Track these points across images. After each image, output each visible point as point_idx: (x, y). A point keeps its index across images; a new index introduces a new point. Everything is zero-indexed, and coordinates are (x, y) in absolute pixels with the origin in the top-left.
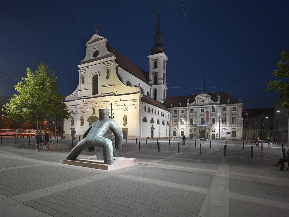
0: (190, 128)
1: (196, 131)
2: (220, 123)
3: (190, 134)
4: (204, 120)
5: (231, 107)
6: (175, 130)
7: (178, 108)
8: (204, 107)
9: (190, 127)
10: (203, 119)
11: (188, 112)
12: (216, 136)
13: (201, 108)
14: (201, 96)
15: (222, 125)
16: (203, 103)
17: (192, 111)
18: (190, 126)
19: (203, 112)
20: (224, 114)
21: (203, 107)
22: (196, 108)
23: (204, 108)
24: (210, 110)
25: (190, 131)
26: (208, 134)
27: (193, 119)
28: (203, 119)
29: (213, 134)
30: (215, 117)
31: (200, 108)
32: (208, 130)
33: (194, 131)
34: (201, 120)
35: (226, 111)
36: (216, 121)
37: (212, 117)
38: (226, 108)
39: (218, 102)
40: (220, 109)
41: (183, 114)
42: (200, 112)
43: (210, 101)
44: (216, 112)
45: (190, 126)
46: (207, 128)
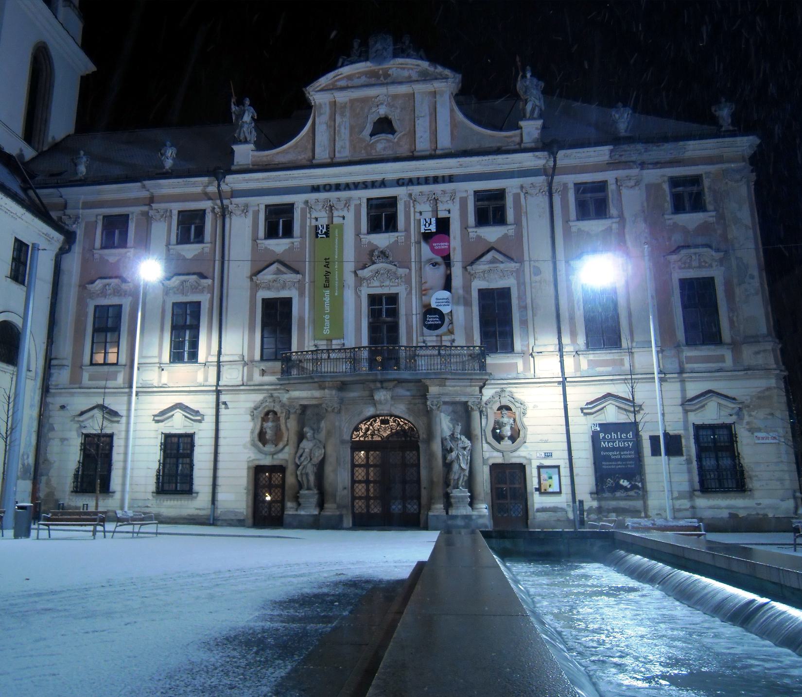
0: (259, 397)
1: (322, 435)
2: (566, 340)
3: (258, 471)
5: (652, 175)
6: (95, 424)
7: (133, 190)
8: (400, 183)
9: (257, 388)
10: (393, 299)
11: (243, 231)
12: (533, 482)
13: (365, 185)
14: (363, 80)
15: (584, 362)
16: (382, 144)
17: (279, 221)
18: (257, 378)
19: (391, 225)
21: (383, 184)
22: (315, 189)
23: (400, 192)
25: (261, 436)
26: (448, 466)
28: (393, 299)
29: (497, 458)
30: (509, 282)
31: (356, 186)
32: (445, 424)
33: (301, 437)
34: (374, 314)
36: (524, 323)
37: (478, 284)
38: (612, 187)
39: (531, 129)
40: (557, 199)
42: (358, 234)
43: (454, 125)
44: (518, 223)
45: (257, 378)
46: (433, 390)
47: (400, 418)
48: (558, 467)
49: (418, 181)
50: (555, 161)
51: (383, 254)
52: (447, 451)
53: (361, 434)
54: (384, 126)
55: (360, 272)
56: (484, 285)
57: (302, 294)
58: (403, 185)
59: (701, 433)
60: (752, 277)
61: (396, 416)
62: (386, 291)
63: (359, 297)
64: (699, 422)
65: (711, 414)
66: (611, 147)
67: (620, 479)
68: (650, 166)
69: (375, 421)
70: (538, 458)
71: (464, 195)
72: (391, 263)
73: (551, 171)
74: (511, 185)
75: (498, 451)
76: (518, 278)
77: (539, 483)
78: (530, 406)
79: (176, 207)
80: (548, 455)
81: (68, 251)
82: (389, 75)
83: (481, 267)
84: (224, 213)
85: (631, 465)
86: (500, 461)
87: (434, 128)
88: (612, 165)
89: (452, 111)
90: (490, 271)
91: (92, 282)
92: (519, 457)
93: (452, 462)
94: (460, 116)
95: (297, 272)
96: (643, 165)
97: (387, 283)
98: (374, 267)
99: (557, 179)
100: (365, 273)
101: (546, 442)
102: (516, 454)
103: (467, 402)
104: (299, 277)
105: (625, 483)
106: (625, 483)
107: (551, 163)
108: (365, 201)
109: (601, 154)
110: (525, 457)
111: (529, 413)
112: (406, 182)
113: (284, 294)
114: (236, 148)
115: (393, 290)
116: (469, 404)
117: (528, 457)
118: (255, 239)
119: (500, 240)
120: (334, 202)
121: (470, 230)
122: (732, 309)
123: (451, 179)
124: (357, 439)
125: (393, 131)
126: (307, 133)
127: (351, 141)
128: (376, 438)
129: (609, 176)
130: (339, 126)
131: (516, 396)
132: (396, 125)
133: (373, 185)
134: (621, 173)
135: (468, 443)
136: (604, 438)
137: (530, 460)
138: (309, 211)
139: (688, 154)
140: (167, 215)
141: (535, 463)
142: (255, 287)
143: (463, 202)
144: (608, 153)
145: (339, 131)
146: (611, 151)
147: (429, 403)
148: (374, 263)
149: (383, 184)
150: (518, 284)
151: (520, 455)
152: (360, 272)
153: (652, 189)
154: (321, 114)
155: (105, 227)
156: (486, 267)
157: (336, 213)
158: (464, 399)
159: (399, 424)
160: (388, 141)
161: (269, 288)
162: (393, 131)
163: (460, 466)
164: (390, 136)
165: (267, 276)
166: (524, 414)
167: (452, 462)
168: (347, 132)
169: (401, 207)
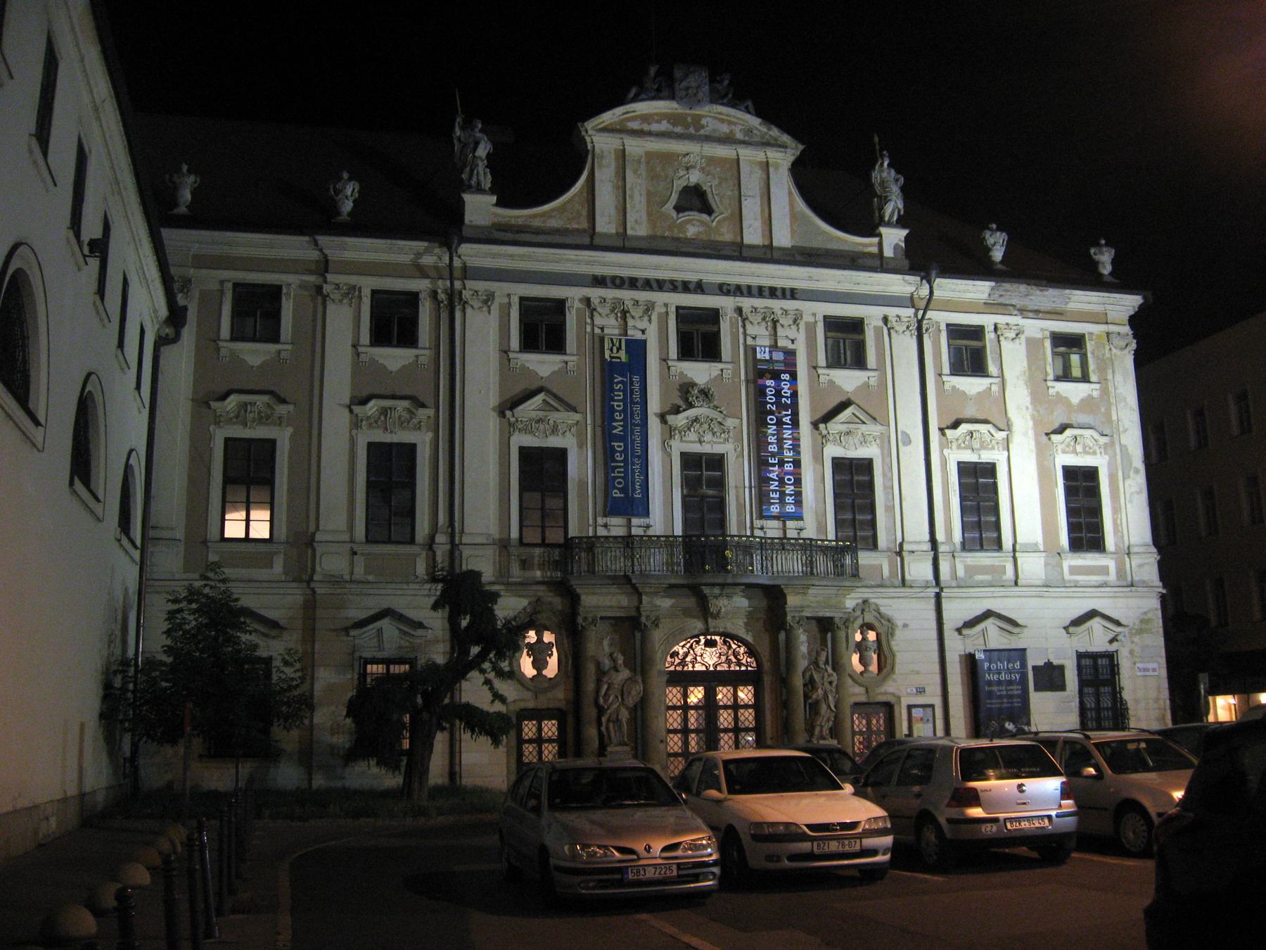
4: (732, 480)
5: (1037, 328)
7: (293, 247)
10: (717, 462)
11: (485, 336)
14: (664, 126)
16: (694, 226)
17: (542, 327)
19: (711, 351)
20: (970, 412)
21: (700, 288)
22: (599, 281)
23: (726, 304)
24: (801, 338)
27: (561, 454)
28: (717, 462)
31: (660, 285)
34: (688, 483)
35: (992, 368)
38: (990, 336)
39: (893, 238)
41: (394, 358)
42: (664, 360)
43: (794, 216)
46: (792, 600)
47: (733, 637)
48: (932, 706)
49: (748, 291)
50: (931, 292)
51: (706, 394)
52: (810, 684)
53: (677, 661)
54: (695, 199)
55: (670, 418)
56: (839, 452)
57: (582, 445)
58: (728, 293)
59: (1083, 662)
60: (1137, 471)
61: (733, 637)
62: (706, 449)
63: (670, 455)
64: (1082, 650)
65: (1096, 638)
66: (993, 284)
67: (1004, 720)
68: (1031, 315)
69: (698, 642)
70: (909, 695)
71: (811, 319)
72: (716, 407)
73: (923, 304)
74: (872, 315)
75: (860, 685)
76: (882, 448)
77: (910, 728)
78: (900, 623)
79: (368, 284)
80: (921, 691)
81: (176, 338)
82: (703, 127)
83: (835, 426)
84: (454, 301)
85: (1017, 703)
86: (863, 699)
87: (767, 215)
88: (990, 307)
89: (790, 193)
90: (848, 433)
91: (224, 397)
92: (885, 693)
93: (817, 702)
94: (801, 205)
95: (574, 410)
96: (1023, 312)
97: (708, 437)
98: (691, 413)
99: (929, 314)
100: (680, 420)
101: (918, 673)
102: (882, 690)
103: (832, 618)
104: (578, 417)
105: (1010, 726)
106: (1010, 726)
107: (925, 291)
108: (674, 309)
109: (979, 289)
110: (893, 694)
111: (899, 634)
112: (732, 289)
113: (554, 442)
114: (467, 198)
115: (718, 449)
116: (837, 621)
117: (896, 692)
118: (505, 351)
119: (858, 389)
120: (629, 304)
121: (820, 371)
122: (1116, 510)
123: (792, 294)
124: (672, 668)
125: (708, 210)
126: (580, 192)
127: (649, 214)
128: (698, 667)
129: (987, 320)
130: (632, 189)
131: (882, 610)
132: (714, 201)
133: (686, 287)
134: (1001, 319)
135: (835, 677)
136: (989, 668)
137: (899, 698)
138: (593, 319)
139: (1072, 306)
140: (352, 293)
141: (905, 702)
142: (509, 428)
143: (811, 329)
144: (987, 290)
145: (632, 197)
146: (993, 289)
147: (789, 618)
148: (691, 406)
149: (700, 288)
150: (882, 454)
151: (889, 689)
152: (670, 418)
153: (1033, 345)
154: (601, 166)
155: (237, 300)
156: (844, 428)
157: (631, 323)
158: (828, 615)
159: (730, 647)
160: (703, 223)
161: (527, 430)
162: (708, 210)
163: (829, 707)
164: (705, 217)
165: (530, 409)
166: (893, 635)
167: (817, 702)
168: (644, 200)
169: (725, 327)
